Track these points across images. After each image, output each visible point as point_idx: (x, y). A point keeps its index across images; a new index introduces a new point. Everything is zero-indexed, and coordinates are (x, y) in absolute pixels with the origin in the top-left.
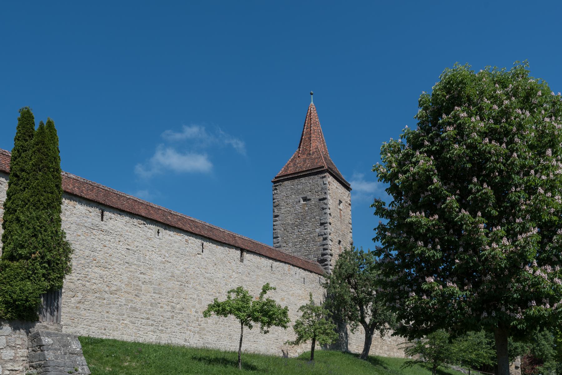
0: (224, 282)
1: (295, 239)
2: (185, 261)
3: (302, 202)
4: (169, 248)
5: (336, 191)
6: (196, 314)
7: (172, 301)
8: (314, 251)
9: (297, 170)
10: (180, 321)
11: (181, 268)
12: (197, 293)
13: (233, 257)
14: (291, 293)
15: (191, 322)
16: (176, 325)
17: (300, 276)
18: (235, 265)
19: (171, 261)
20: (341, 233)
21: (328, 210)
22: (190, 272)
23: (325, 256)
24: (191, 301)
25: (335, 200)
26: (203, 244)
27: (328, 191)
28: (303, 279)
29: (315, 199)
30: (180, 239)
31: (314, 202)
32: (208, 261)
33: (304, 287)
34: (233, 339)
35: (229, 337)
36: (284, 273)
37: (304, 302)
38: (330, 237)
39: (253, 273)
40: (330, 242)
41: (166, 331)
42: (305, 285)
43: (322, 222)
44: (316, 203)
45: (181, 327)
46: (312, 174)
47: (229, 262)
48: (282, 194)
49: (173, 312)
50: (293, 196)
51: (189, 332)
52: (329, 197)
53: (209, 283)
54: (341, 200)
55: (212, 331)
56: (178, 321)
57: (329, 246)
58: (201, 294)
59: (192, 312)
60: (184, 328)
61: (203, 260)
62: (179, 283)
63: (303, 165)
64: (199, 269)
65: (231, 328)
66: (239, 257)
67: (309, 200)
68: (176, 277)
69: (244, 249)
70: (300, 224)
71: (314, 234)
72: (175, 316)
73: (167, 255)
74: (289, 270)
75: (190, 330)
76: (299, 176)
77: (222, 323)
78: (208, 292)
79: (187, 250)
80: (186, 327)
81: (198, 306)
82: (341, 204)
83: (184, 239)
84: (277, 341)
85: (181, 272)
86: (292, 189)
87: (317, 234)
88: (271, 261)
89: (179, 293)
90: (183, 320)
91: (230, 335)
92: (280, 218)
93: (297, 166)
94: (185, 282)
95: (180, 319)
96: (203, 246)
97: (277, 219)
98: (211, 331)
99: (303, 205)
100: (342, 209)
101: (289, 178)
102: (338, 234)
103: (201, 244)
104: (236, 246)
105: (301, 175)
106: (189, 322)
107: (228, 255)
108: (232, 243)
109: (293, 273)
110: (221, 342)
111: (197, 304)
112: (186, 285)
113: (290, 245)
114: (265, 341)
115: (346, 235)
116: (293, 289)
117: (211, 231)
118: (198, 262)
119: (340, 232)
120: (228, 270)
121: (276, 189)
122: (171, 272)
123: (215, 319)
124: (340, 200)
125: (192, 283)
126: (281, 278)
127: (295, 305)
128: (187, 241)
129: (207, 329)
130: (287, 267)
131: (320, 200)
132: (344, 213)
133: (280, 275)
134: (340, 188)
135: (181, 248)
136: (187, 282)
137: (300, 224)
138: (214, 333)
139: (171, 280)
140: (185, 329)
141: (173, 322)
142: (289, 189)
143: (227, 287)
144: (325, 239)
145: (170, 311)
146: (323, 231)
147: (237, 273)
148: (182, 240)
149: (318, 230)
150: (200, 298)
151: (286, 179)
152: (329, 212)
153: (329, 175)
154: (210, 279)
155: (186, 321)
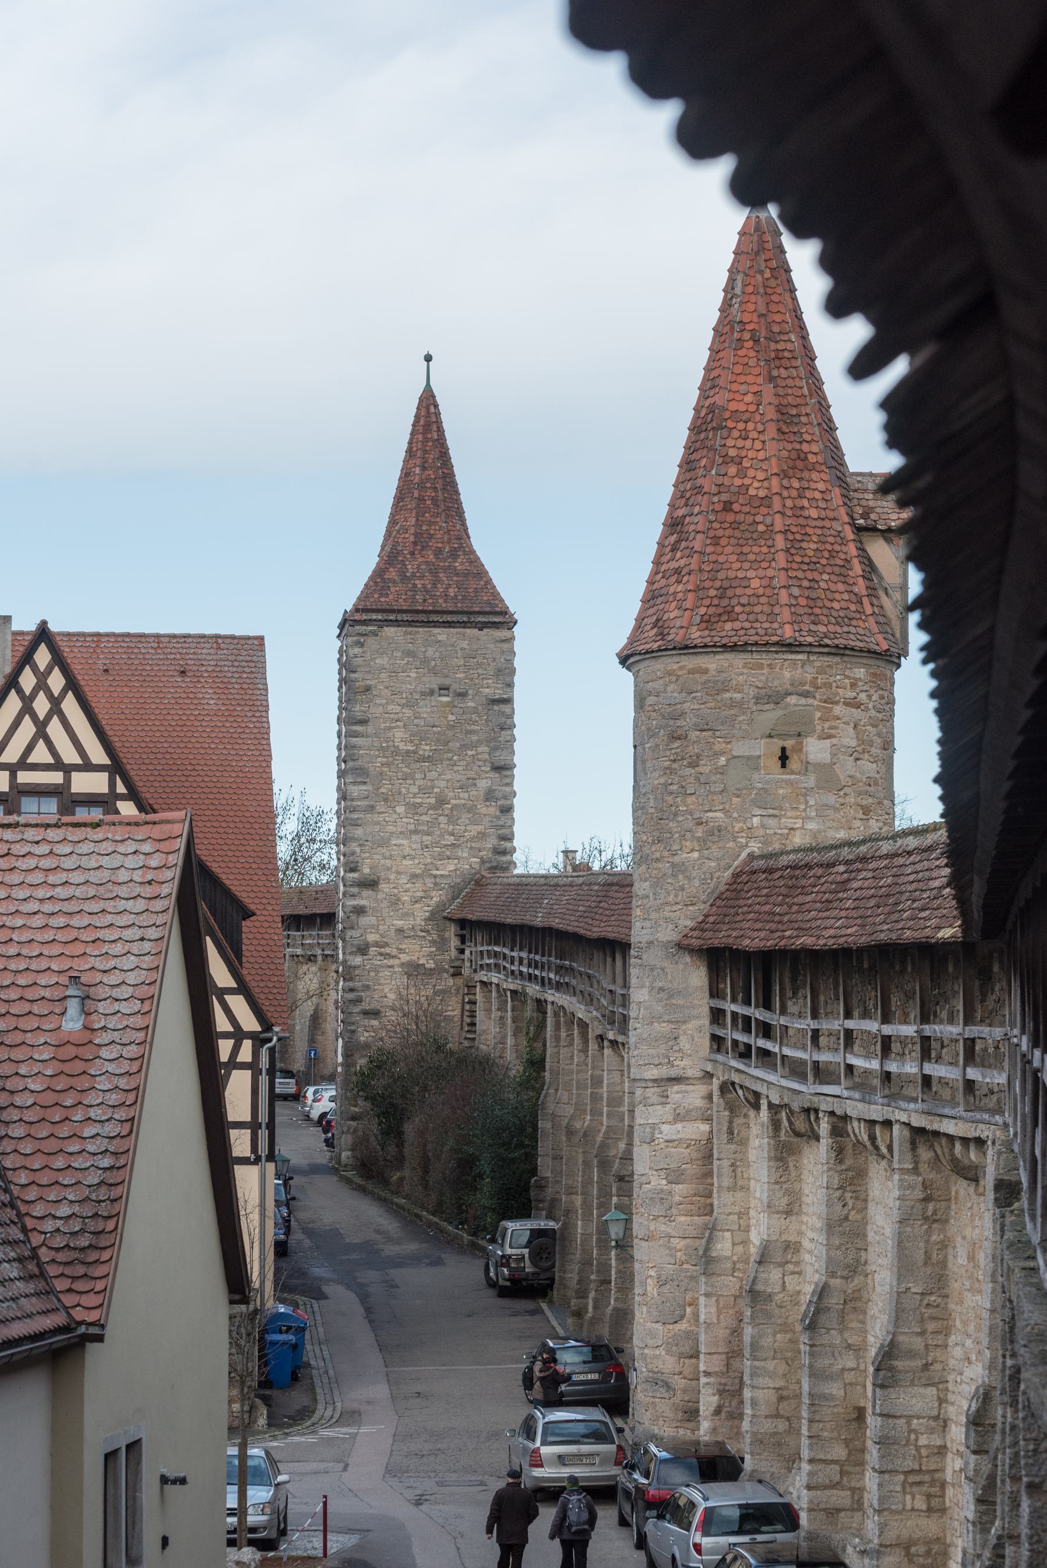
1: (415, 796)
8: (472, 839)
31: (472, 704)
44: (480, 708)
50: (413, 675)
63: (434, 585)
67: (463, 695)
70: (428, 759)
87: (482, 793)
92: (370, 729)
113: (400, 809)
121: (362, 645)
137: (428, 759)
142: (399, 654)
149: (483, 784)
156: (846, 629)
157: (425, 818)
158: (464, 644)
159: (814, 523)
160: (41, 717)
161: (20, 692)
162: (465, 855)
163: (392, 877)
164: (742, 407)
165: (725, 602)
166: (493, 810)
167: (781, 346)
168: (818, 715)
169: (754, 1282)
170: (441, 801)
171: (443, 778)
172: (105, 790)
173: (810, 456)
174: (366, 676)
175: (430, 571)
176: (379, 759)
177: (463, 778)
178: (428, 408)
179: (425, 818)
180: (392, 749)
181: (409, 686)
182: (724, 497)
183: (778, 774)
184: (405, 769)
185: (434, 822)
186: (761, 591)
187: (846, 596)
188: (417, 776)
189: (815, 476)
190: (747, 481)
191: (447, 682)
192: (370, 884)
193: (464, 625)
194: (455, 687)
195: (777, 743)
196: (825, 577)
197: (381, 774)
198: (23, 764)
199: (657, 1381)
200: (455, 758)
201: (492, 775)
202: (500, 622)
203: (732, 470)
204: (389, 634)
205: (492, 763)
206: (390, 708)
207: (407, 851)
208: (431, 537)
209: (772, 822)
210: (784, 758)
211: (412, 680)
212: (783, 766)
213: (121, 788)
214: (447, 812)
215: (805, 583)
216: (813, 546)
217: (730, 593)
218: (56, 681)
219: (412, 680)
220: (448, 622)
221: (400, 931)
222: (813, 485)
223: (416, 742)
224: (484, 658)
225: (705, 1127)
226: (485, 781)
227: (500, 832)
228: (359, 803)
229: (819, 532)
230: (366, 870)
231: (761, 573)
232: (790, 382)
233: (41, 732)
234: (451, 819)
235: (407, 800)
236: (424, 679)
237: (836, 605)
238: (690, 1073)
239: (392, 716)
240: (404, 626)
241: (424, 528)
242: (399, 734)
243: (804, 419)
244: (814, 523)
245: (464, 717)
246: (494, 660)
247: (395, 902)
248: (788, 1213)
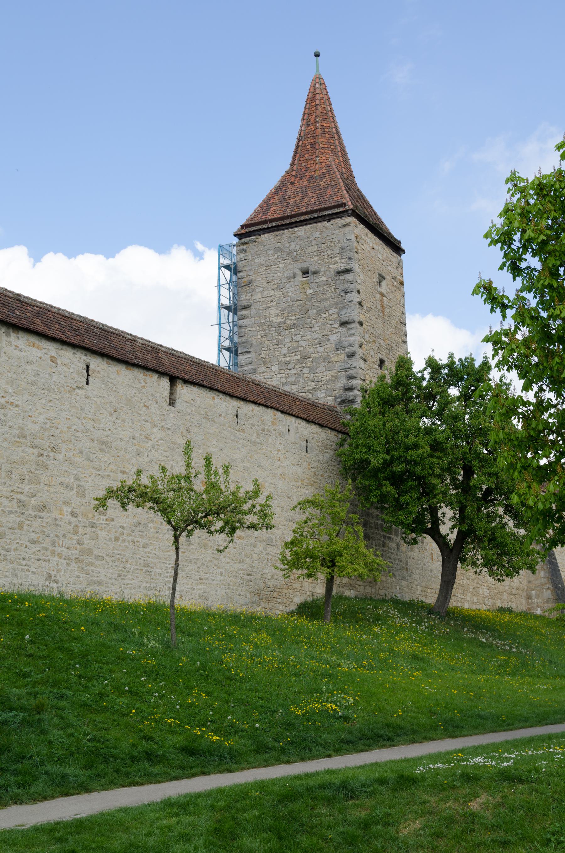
0: (134, 448)
2: (50, 404)
3: (300, 278)
4: (15, 376)
5: (373, 254)
6: (73, 519)
7: (19, 490)
8: (328, 382)
9: (289, 212)
10: (38, 535)
11: (41, 419)
12: (75, 472)
13: (153, 395)
14: (279, 472)
15: (61, 536)
16: (27, 543)
17: (298, 435)
18: (159, 412)
19: (19, 403)
20: (384, 344)
21: (357, 295)
22: (59, 427)
23: (351, 393)
24: (63, 491)
25: (369, 273)
26: (88, 367)
27: (356, 254)
28: (305, 442)
29: (328, 273)
30: (40, 355)
31: (325, 279)
32: (99, 403)
33: (307, 459)
34: (153, 573)
35: (145, 569)
36: (263, 430)
37: (307, 492)
38: (360, 352)
39: (196, 430)
40: (362, 364)
41: (5, 556)
42: (309, 456)
43: (344, 319)
45: (38, 547)
46: (319, 219)
47: (145, 406)
48: (256, 261)
49: (23, 514)
50: (281, 266)
51: (56, 558)
52: (356, 267)
53: (102, 450)
54: (384, 274)
55: (107, 555)
56: (33, 534)
57: (360, 371)
58: (83, 475)
59: (64, 515)
60: (47, 549)
61: (88, 401)
62: (36, 451)
63: (302, 200)
64: (79, 422)
65: (147, 550)
66: (166, 393)
67: (315, 273)
68: (28, 438)
69: (178, 378)
71: (328, 346)
72: (27, 522)
73: (10, 390)
74: (273, 423)
75: (58, 554)
76: (293, 223)
77: (130, 538)
78: (99, 470)
79: (54, 379)
80: (51, 548)
81: (76, 501)
82: (384, 283)
83: (48, 356)
84: (249, 577)
85: (41, 427)
87: (333, 345)
88: (235, 403)
89: (36, 472)
90: (43, 532)
91: (147, 565)
92: (252, 311)
93: (289, 203)
94: (49, 449)
95: (37, 530)
96: (87, 371)
97: (244, 312)
98: (104, 555)
99: (304, 283)
100: (384, 292)
101: (272, 227)
102: (378, 345)
103: (85, 367)
104: (161, 370)
105: (296, 222)
106: (57, 536)
107: (144, 390)
108: (152, 364)
109: (283, 430)
110: (126, 581)
111: (75, 497)
112: (52, 454)
113: (275, 368)
114: (222, 578)
115: (395, 347)
116: (284, 465)
117: (106, 339)
118: (77, 405)
119: (382, 342)
120: (144, 422)
121: (245, 251)
122: (19, 427)
123: (114, 530)
124: (380, 275)
125: (63, 450)
126: (258, 440)
127: (289, 498)
128: (53, 359)
129: (96, 552)
130: (269, 415)
131: (340, 273)
132: (389, 300)
133: (255, 435)
134: (381, 249)
135: (42, 375)
136: (54, 449)
138: (112, 561)
139: (18, 444)
140: (48, 553)
141: (22, 537)
142: (271, 252)
143: (140, 459)
144: (351, 355)
145: (16, 512)
146: (347, 339)
147: (163, 429)
148: (43, 358)
149: (334, 338)
150: (82, 483)
151: (264, 229)
152: (358, 300)
153: (358, 222)
154: (103, 443)
155: (52, 535)
157: (293, 372)
158: (317, 235)
162: (323, 395)
166: (342, 356)
174: (249, 273)
176: (259, 333)
177: (320, 336)
178: (314, 86)
179: (293, 372)
180: (268, 323)
181: (279, 274)
184: (277, 337)
185: (300, 374)
188: (286, 340)
191: (305, 265)
194: (312, 269)
197: (261, 344)
200: (313, 322)
201: (341, 330)
202: (340, 212)
204: (264, 239)
205: (340, 321)
206: (266, 293)
208: (307, 169)
214: (308, 365)
220: (304, 221)
223: (285, 315)
224: (331, 242)
226: (335, 335)
227: (348, 373)
228: (246, 368)
234: (312, 370)
235: (280, 360)
236: (289, 267)
239: (267, 299)
240: (274, 231)
241: (303, 164)
242: (273, 311)
245: (319, 289)
246: (339, 241)
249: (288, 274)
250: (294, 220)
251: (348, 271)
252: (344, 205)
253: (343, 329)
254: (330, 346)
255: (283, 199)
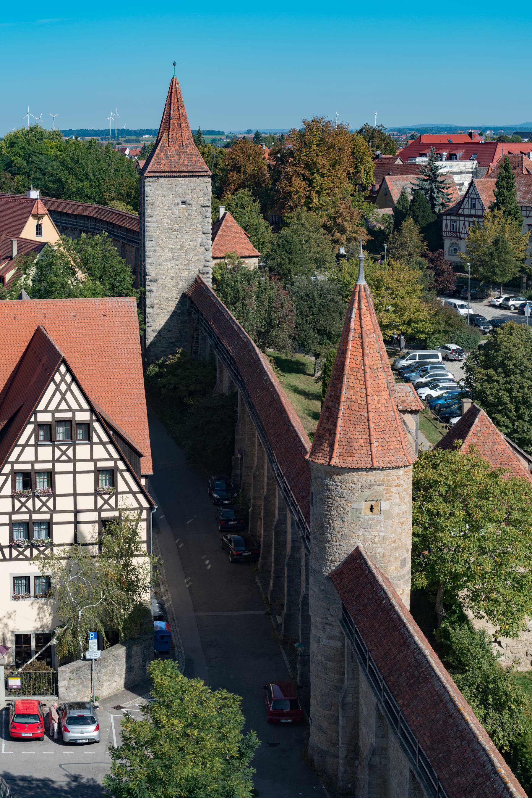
63: (179, 160)
70: (178, 230)
86: (169, 189)
92: (155, 219)
97: (150, 219)
121: (150, 186)
137: (178, 230)
149: (199, 240)
156: (396, 457)
158: (192, 184)
159: (384, 414)
160: (63, 392)
161: (55, 383)
163: (164, 277)
164: (355, 366)
165: (349, 448)
166: (203, 250)
167: (371, 339)
168: (385, 492)
169: (370, 761)
170: (182, 247)
171: (183, 238)
172: (88, 418)
173: (382, 385)
175: (177, 154)
179: (176, 254)
182: (349, 403)
183: (370, 515)
185: (179, 256)
186: (363, 445)
187: (396, 443)
189: (383, 393)
190: (357, 397)
191: (184, 200)
192: (155, 281)
193: (191, 176)
194: (188, 202)
195: (369, 503)
196: (388, 436)
198: (57, 410)
199: (319, 728)
203: (352, 392)
207: (169, 267)
209: (366, 533)
210: (372, 509)
211: (171, 199)
212: (372, 511)
213: (94, 418)
215: (381, 440)
216: (383, 424)
217: (351, 444)
218: (68, 378)
219: (171, 199)
221: (167, 298)
222: (383, 398)
225: (340, 644)
229: (385, 417)
230: (153, 275)
231: (364, 437)
232: (374, 355)
233: (63, 398)
237: (392, 447)
238: (334, 623)
242: (166, 221)
243: (379, 370)
244: (384, 414)
247: (165, 288)
248: (383, 737)
249: (174, 202)
250: (179, 174)
251: (207, 206)
252: (206, 172)
253: (203, 236)
254: (197, 243)
255: (167, 157)
